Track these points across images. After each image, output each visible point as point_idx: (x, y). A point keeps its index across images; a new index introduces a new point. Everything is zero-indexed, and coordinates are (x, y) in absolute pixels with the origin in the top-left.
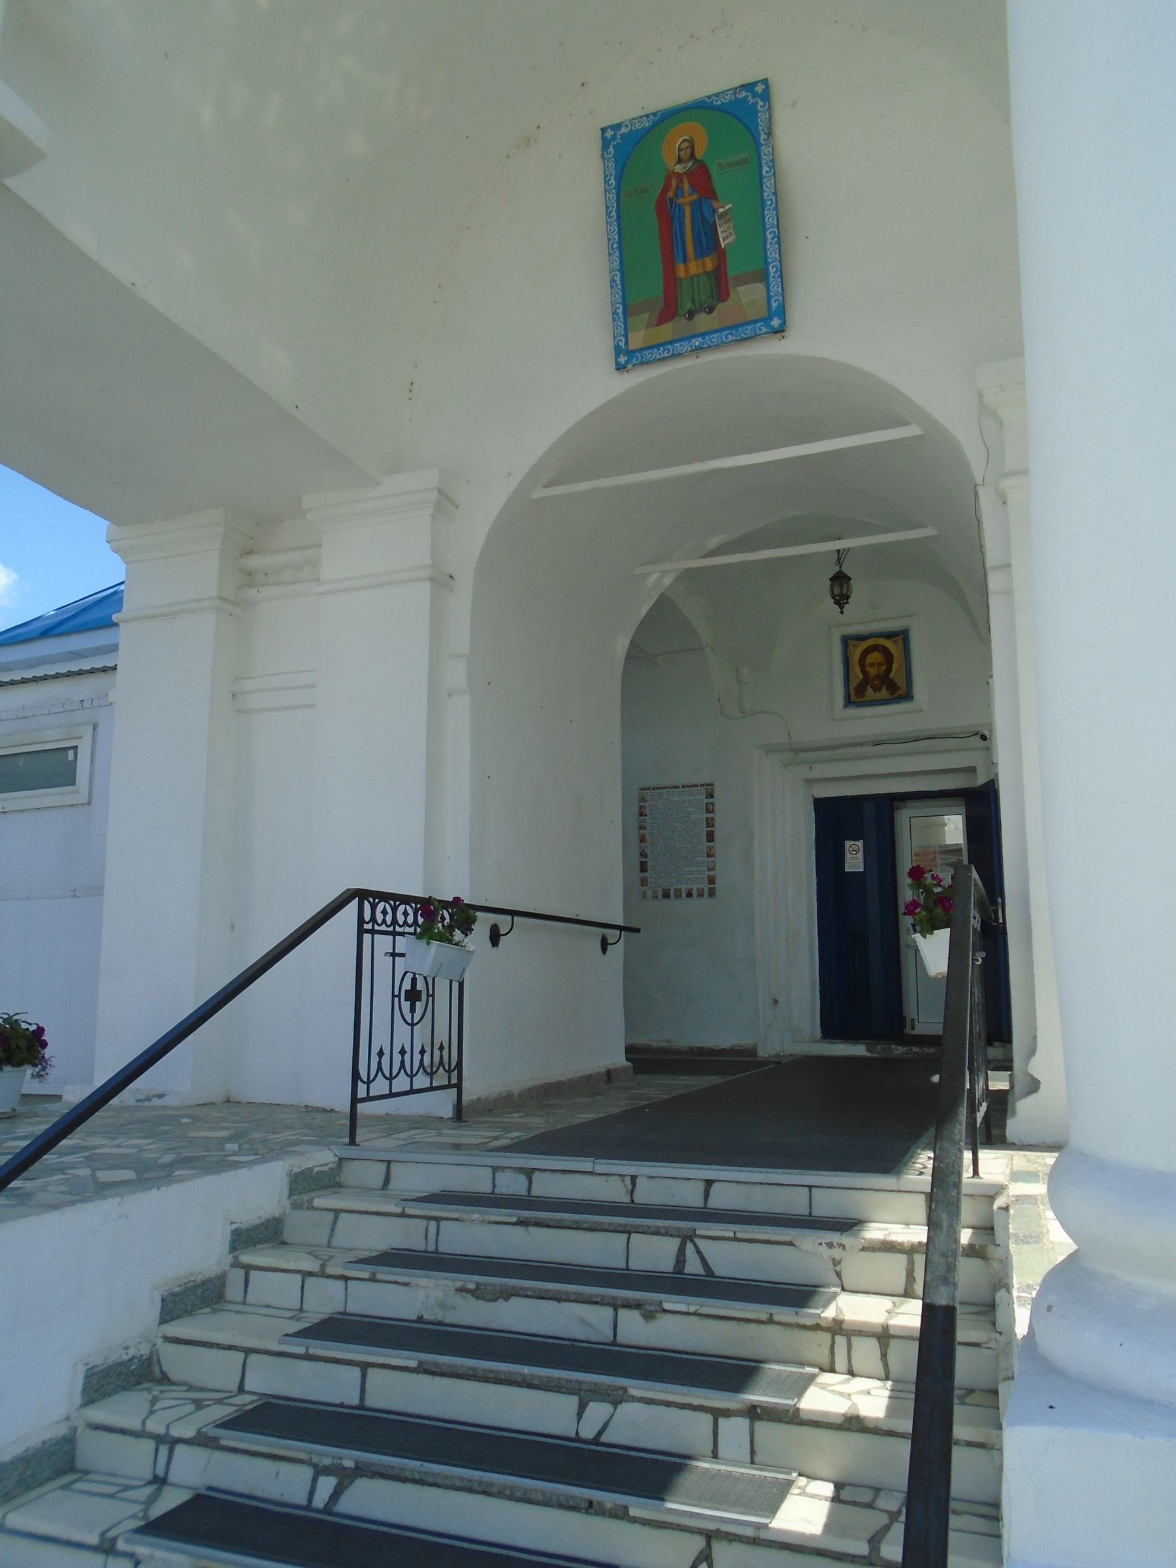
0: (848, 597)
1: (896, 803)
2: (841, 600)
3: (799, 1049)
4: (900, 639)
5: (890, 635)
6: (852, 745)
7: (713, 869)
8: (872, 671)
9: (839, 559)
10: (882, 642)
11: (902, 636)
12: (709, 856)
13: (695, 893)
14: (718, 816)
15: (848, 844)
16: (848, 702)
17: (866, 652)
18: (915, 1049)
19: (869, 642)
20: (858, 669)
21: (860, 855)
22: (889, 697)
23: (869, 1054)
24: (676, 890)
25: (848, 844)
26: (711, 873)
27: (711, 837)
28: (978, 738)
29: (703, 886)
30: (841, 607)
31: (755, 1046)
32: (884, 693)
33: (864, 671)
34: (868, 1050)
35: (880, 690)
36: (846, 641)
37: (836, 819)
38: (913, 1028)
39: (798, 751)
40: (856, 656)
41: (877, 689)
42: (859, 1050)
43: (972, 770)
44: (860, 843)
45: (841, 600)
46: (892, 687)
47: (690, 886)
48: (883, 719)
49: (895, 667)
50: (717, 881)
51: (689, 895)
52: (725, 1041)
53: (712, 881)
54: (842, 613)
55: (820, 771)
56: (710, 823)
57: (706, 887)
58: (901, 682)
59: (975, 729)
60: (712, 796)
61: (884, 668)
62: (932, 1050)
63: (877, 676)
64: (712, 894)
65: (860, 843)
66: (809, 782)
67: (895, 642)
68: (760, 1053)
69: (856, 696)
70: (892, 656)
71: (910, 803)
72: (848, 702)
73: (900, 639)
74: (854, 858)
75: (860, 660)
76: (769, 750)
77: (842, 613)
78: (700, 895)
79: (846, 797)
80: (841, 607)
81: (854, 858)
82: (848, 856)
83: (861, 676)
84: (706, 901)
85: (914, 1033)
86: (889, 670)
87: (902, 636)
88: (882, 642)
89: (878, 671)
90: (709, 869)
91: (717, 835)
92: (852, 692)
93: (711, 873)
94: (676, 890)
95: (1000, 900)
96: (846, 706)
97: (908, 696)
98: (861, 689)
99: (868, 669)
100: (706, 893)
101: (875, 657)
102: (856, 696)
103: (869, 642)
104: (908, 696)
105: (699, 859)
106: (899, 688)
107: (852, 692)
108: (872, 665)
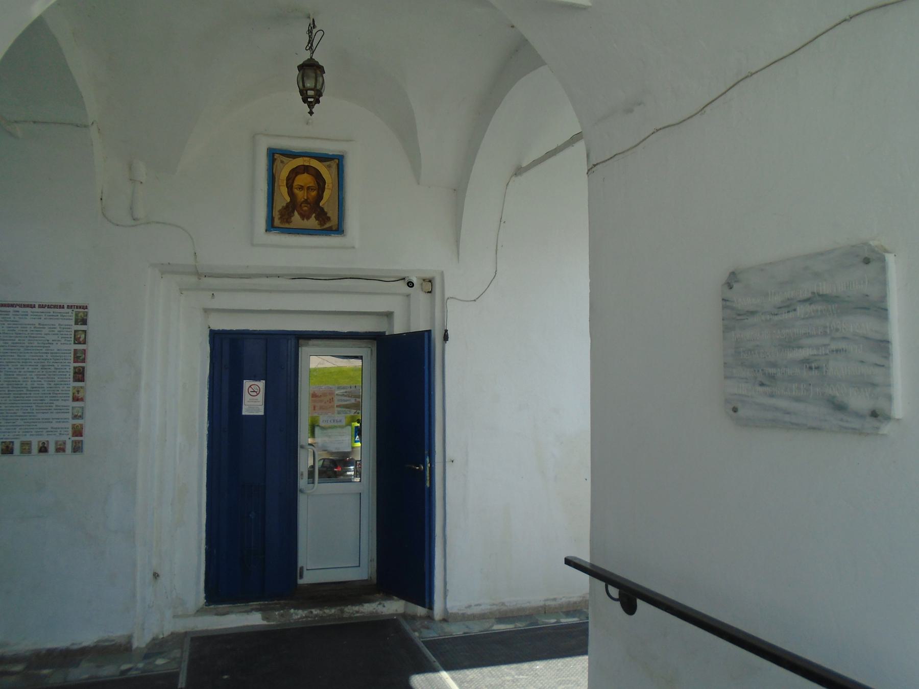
0: (321, 95)
1: (301, 341)
4: (333, 164)
5: (323, 158)
7: (81, 417)
8: (301, 195)
9: (311, 42)
10: (315, 163)
11: (337, 161)
12: (75, 399)
13: (52, 448)
14: (92, 348)
15: (247, 384)
17: (295, 172)
18: (315, 612)
19: (299, 162)
20: (284, 190)
21: (261, 398)
22: (318, 227)
23: (265, 623)
24: (23, 444)
25: (247, 384)
26: (78, 422)
27: (79, 375)
29: (63, 438)
30: (311, 105)
31: (130, 637)
32: (312, 222)
34: (264, 618)
35: (308, 218)
36: (274, 155)
37: (233, 357)
38: (301, 577)
39: (199, 274)
40: (284, 174)
41: (304, 216)
43: (389, 315)
44: (261, 384)
46: (322, 216)
47: (44, 439)
50: (86, 431)
51: (43, 449)
52: (88, 638)
53: (78, 432)
54: (311, 113)
55: (224, 301)
56: (79, 357)
57: (69, 440)
58: (332, 213)
59: (403, 275)
60: (84, 322)
61: (314, 193)
62: (333, 611)
63: (306, 201)
64: (77, 448)
65: (261, 384)
66: (206, 311)
67: (329, 167)
68: (135, 644)
69: (281, 219)
70: (324, 183)
71: (312, 342)
72: (271, 226)
73: (333, 164)
74: (253, 400)
75: (288, 179)
76: (167, 269)
77: (311, 113)
78: (60, 449)
80: (311, 105)
81: (253, 400)
82: (246, 398)
83: (288, 199)
84: (69, 456)
86: (320, 197)
87: (337, 161)
88: (315, 163)
89: (306, 196)
90: (75, 417)
91: (89, 373)
92: (276, 215)
93: (78, 422)
94: (23, 444)
97: (339, 230)
98: (287, 213)
99: (296, 191)
100: (69, 447)
101: (304, 179)
103: (299, 162)
104: (339, 230)
105: (60, 403)
106: (329, 219)
107: (276, 215)
108: (301, 188)
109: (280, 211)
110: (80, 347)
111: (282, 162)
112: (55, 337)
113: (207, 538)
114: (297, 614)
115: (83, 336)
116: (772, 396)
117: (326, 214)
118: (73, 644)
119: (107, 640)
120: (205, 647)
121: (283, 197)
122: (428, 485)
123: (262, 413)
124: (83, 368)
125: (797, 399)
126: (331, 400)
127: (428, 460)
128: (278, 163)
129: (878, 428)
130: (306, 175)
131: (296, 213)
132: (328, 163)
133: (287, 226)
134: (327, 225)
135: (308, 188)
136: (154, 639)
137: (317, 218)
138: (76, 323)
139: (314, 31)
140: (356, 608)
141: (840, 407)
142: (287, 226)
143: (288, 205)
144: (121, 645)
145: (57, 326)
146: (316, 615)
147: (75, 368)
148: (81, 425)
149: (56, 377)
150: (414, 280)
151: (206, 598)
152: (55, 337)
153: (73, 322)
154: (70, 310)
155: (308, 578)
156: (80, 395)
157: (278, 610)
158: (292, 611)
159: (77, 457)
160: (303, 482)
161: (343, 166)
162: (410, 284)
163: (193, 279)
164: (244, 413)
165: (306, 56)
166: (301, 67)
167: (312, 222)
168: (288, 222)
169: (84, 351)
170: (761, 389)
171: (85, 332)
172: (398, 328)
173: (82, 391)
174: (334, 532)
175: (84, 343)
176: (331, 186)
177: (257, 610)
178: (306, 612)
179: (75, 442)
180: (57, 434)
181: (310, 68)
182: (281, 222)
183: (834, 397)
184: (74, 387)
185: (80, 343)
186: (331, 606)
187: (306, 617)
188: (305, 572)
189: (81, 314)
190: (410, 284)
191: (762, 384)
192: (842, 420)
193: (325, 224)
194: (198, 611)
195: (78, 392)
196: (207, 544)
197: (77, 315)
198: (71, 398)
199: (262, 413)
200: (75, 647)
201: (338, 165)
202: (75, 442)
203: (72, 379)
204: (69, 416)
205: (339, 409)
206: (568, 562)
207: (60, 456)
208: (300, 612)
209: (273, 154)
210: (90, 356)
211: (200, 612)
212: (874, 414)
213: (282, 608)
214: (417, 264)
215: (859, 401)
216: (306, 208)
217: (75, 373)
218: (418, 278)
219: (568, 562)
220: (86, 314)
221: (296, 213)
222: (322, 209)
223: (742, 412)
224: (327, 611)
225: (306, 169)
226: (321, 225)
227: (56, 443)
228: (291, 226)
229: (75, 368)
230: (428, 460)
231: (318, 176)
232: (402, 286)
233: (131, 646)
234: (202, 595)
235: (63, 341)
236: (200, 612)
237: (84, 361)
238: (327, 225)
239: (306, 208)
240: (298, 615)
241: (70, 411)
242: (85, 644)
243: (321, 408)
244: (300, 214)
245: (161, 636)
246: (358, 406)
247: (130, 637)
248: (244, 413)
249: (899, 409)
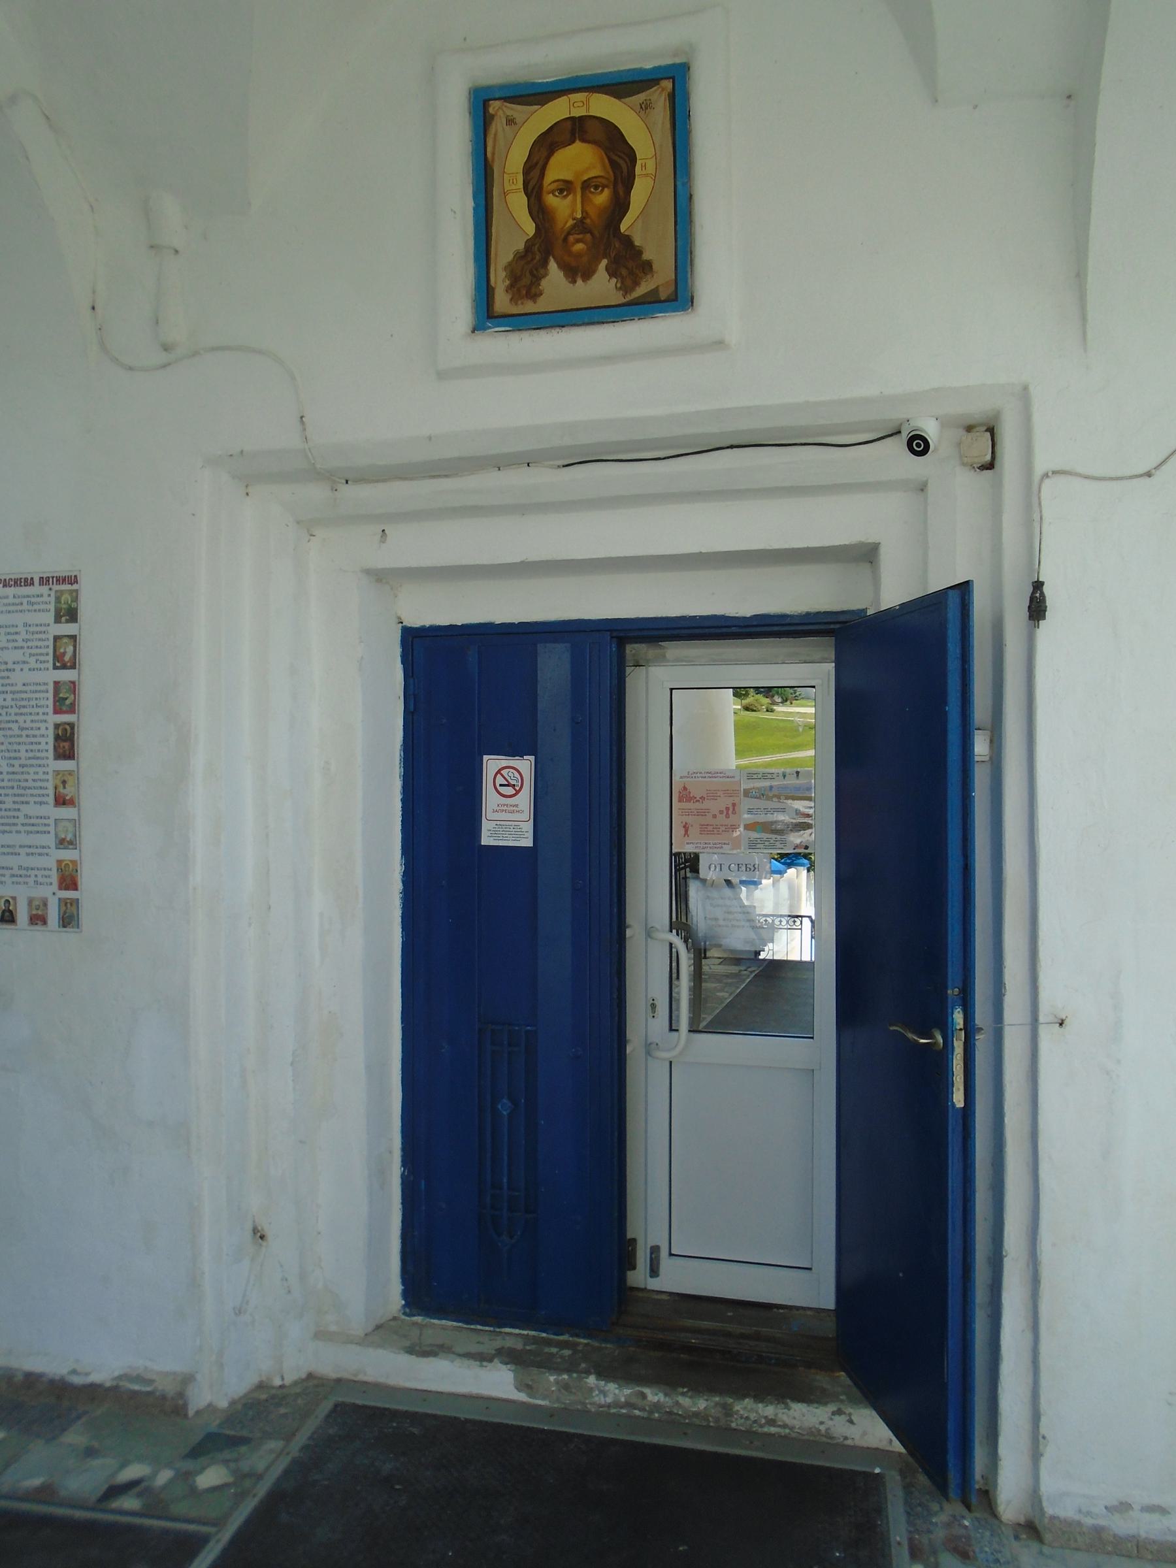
1: (631, 649)
4: (658, 97)
6: (500, 463)
8: (564, 209)
10: (603, 107)
11: (667, 86)
12: (61, 801)
13: (22, 915)
14: (90, 679)
15: (492, 764)
16: (487, 315)
18: (654, 1396)
20: (518, 203)
22: (617, 298)
23: (522, 1397)
25: (492, 764)
26: (67, 855)
27: (66, 743)
28: (898, 447)
31: (188, 1379)
32: (601, 286)
33: (539, 211)
34: (521, 1386)
35: (587, 275)
36: (485, 106)
37: (466, 690)
38: (654, 1272)
40: (514, 158)
41: (577, 271)
43: (867, 555)
46: (628, 261)
48: (592, 375)
49: (639, 194)
52: (100, 1359)
53: (69, 881)
55: (412, 547)
57: (52, 894)
58: (657, 249)
59: (895, 415)
60: (71, 614)
61: (602, 198)
62: (701, 1404)
63: (581, 226)
64: (69, 919)
65: (525, 765)
66: (381, 577)
67: (646, 107)
69: (511, 294)
70: (631, 156)
71: (674, 650)
72: (487, 315)
73: (658, 97)
74: (507, 808)
75: (529, 168)
76: (252, 472)
78: (38, 919)
79: (490, 625)
81: (507, 808)
82: (491, 800)
83: (530, 228)
84: (52, 936)
85: (654, 1284)
86: (620, 206)
87: (667, 86)
88: (603, 107)
89: (583, 207)
90: (62, 843)
91: (86, 741)
92: (499, 280)
93: (67, 855)
95: (958, 1017)
96: (478, 328)
97: (678, 297)
99: (552, 200)
101: (576, 160)
102: (511, 294)
104: (678, 297)
106: (647, 267)
107: (499, 280)
108: (565, 187)
109: (511, 269)
110: (66, 675)
111: (510, 121)
112: (18, 655)
113: (404, 1149)
114: (604, 1393)
115: (70, 649)
117: (639, 252)
118: (74, 1372)
119: (139, 1379)
120: (366, 1432)
121: (517, 224)
122: (958, 1099)
123: (527, 842)
124: (72, 725)
130: (578, 148)
131: (553, 265)
132: (641, 97)
133: (529, 307)
135: (586, 185)
136: (261, 1386)
137: (612, 273)
138: (58, 620)
140: (769, 1410)
142: (529, 307)
143: (529, 245)
144: (164, 1397)
145: (21, 629)
146: (657, 1406)
147: (57, 726)
148: (74, 862)
149: (23, 748)
150: (931, 430)
151: (405, 1294)
152: (18, 655)
153: (51, 617)
154: (44, 590)
156: (69, 792)
157: (557, 1370)
158: (592, 1380)
159: (69, 937)
160: (645, 1025)
161: (686, 97)
162: (918, 445)
163: (316, 493)
164: (486, 840)
169: (73, 686)
171: (73, 638)
172: (894, 590)
173: (71, 781)
174: (732, 1171)
175: (73, 667)
176: (651, 165)
177: (511, 1357)
178: (627, 1391)
179: (64, 902)
180: (31, 880)
184: (57, 773)
185: (64, 667)
186: (697, 1389)
187: (628, 1405)
188: (665, 1263)
189: (66, 597)
190: (918, 445)
193: (636, 284)
194: (378, 1327)
195: (64, 782)
196: (404, 1163)
197: (58, 600)
198: (51, 800)
199: (527, 842)
200: (77, 1380)
201: (672, 97)
202: (64, 902)
203: (51, 754)
204: (50, 840)
205: (754, 835)
207: (38, 932)
208: (612, 1387)
209: (486, 103)
210: (87, 697)
211: (382, 1333)
213: (570, 1367)
216: (580, 246)
217: (57, 738)
220: (75, 596)
221: (553, 265)
222: (627, 241)
224: (685, 1401)
225: (577, 129)
226: (625, 289)
227: (30, 902)
228: (541, 305)
229: (57, 726)
231: (613, 144)
233: (185, 1406)
234: (395, 1287)
235: (33, 665)
237: (72, 709)
239: (580, 246)
240: (608, 1398)
241: (52, 829)
242: (95, 1378)
243: (705, 829)
244: (563, 266)
245: (277, 1382)
247: (188, 1379)
248: (486, 840)
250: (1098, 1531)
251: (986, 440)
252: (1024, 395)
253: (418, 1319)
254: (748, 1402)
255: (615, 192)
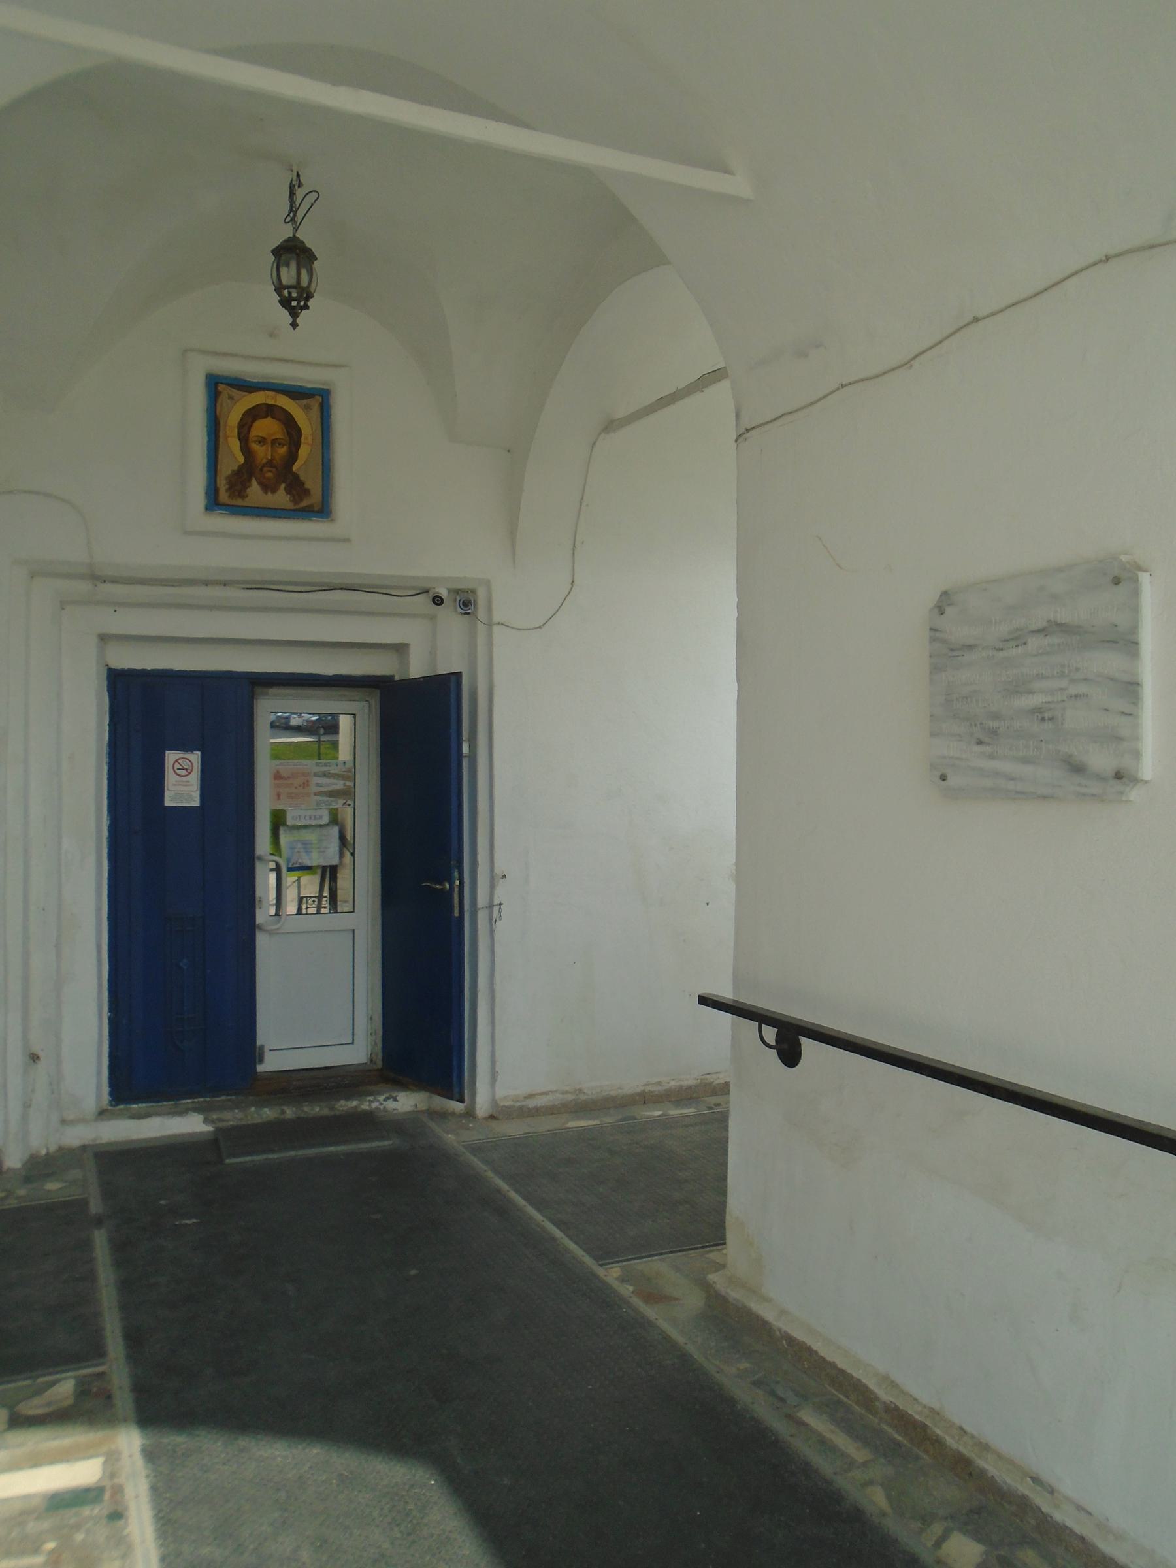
0: (309, 296)
1: (258, 690)
2: (294, 301)
3: (76, 1136)
4: (315, 403)
5: (298, 394)
6: (207, 583)
8: (262, 453)
9: (293, 210)
10: (284, 402)
11: (319, 399)
15: (171, 756)
17: (253, 414)
19: (258, 398)
20: (235, 444)
21: (195, 778)
22: (290, 506)
25: (171, 756)
34: (206, 1121)
35: (274, 491)
36: (216, 385)
37: (148, 711)
38: (261, 1061)
39: (96, 577)
40: (233, 417)
41: (267, 487)
42: (188, 1124)
43: (400, 649)
44: (195, 757)
45: (294, 301)
46: (297, 488)
48: (270, 545)
49: (304, 452)
54: (294, 325)
58: (313, 483)
59: (427, 585)
61: (283, 451)
63: (270, 463)
65: (195, 757)
66: (104, 638)
67: (307, 408)
69: (230, 491)
72: (214, 502)
73: (315, 403)
74: (182, 782)
77: (294, 325)
79: (171, 671)
81: (182, 782)
82: (171, 779)
83: (241, 459)
86: (293, 457)
87: (319, 399)
88: (284, 402)
89: (269, 454)
96: (208, 508)
97: (322, 510)
99: (255, 447)
101: (266, 427)
102: (230, 491)
103: (258, 398)
104: (322, 510)
106: (307, 492)
108: (262, 441)
109: (228, 478)
111: (231, 398)
116: (992, 757)
117: (303, 484)
123: (196, 803)
125: (1026, 761)
126: (306, 784)
127: (456, 874)
128: (223, 399)
129: (1122, 793)
130: (269, 421)
131: (254, 482)
132: (305, 402)
133: (239, 502)
134: (304, 504)
135: (274, 441)
139: (300, 193)
140: (355, 1103)
141: (1077, 768)
142: (239, 502)
143: (241, 467)
150: (443, 593)
151: (111, 1094)
155: (270, 1064)
161: (329, 407)
163: (83, 587)
164: (168, 802)
165: (286, 232)
166: (277, 252)
167: (281, 498)
168: (242, 494)
170: (978, 749)
172: (417, 669)
174: (313, 992)
176: (310, 438)
177: (198, 1110)
181: (293, 252)
182: (231, 496)
183: (1070, 756)
190: (438, 600)
191: (980, 743)
192: (1080, 785)
193: (302, 500)
196: (110, 1010)
199: (196, 803)
201: (322, 406)
205: (319, 798)
206: (704, 1000)
209: (216, 384)
211: (102, 1114)
212: (1118, 776)
214: (445, 567)
215: (1100, 760)
216: (269, 475)
218: (449, 591)
219: (704, 1000)
221: (254, 482)
222: (296, 477)
223: (953, 781)
225: (269, 411)
226: (295, 502)
228: (247, 502)
230: (456, 874)
231: (289, 422)
232: (423, 601)
234: (106, 1090)
236: (102, 1114)
238: (304, 504)
239: (269, 475)
243: (290, 796)
244: (260, 483)
246: (348, 794)
248: (168, 802)
249: (1148, 769)
250: (521, 1108)
251: (466, 603)
252: (488, 584)
253: (122, 1107)
254: (342, 1102)
255: (290, 448)
